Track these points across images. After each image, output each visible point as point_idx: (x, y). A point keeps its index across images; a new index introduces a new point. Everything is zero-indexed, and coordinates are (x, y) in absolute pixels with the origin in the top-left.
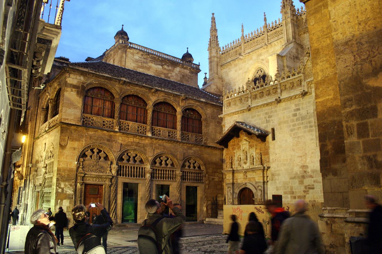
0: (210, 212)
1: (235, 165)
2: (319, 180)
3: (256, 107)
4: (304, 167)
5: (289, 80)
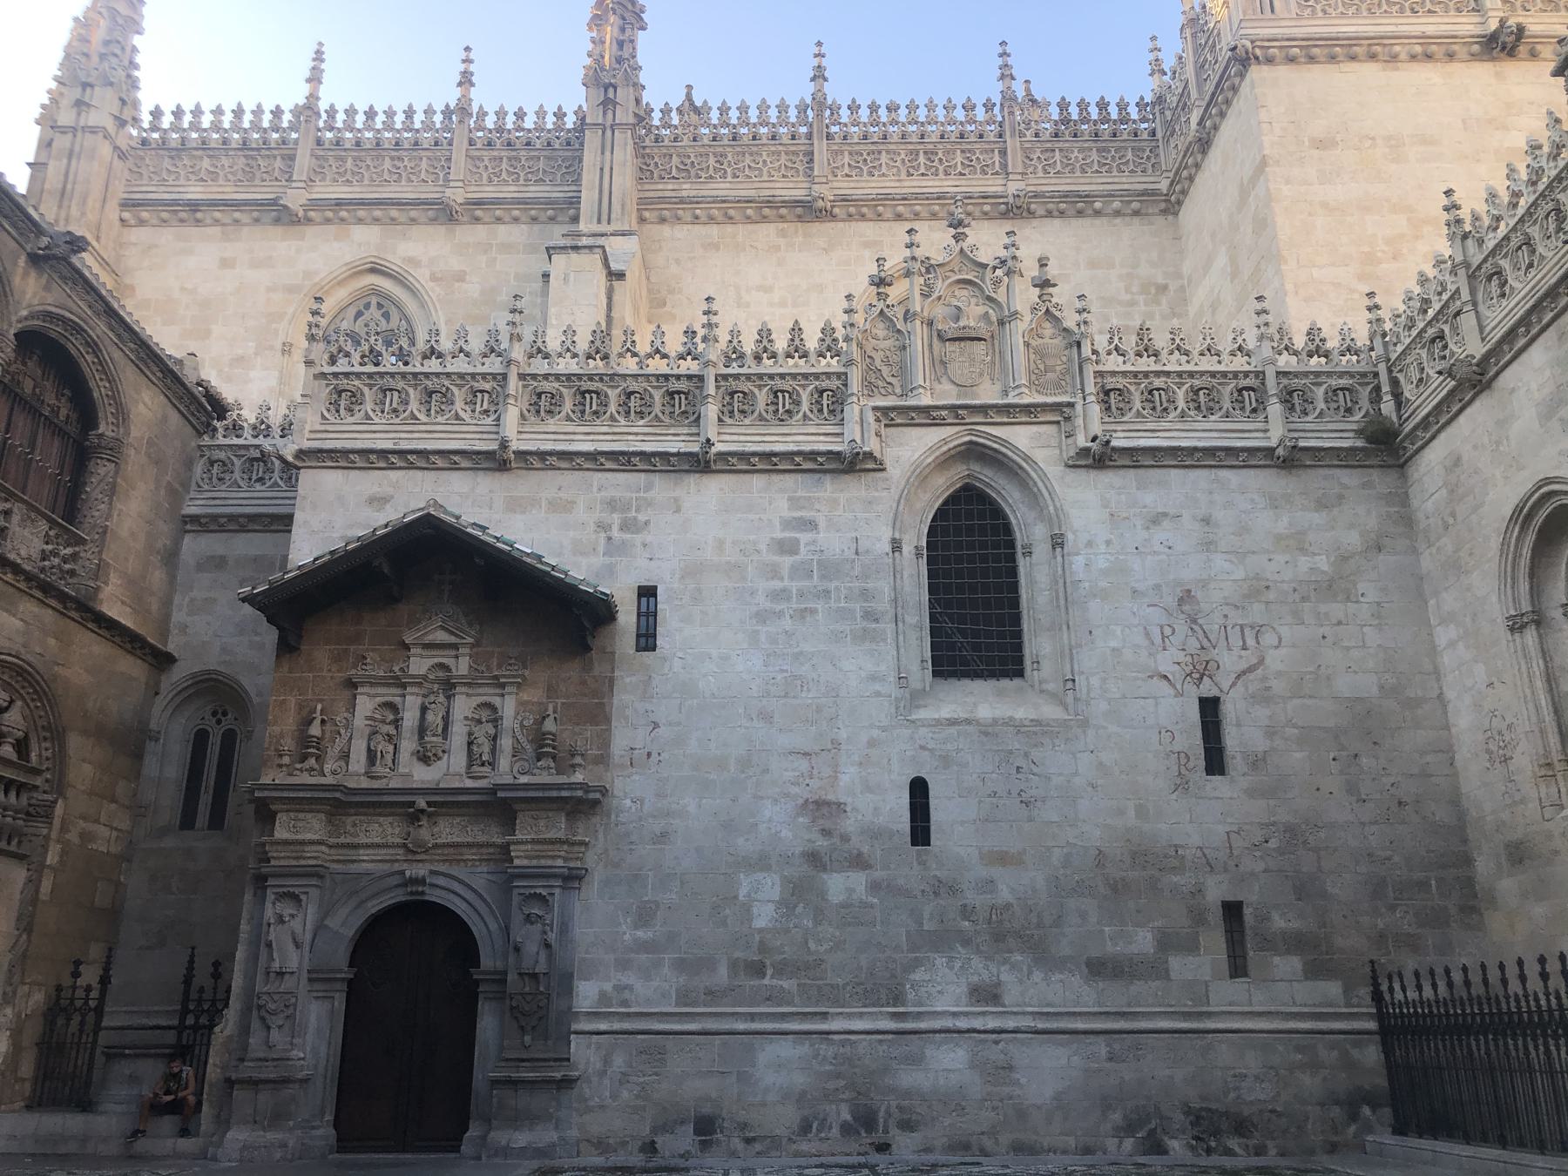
0: (27, 1069)
1: (345, 756)
2: (901, 881)
3: (552, 460)
4: (822, 809)
5: (771, 377)
